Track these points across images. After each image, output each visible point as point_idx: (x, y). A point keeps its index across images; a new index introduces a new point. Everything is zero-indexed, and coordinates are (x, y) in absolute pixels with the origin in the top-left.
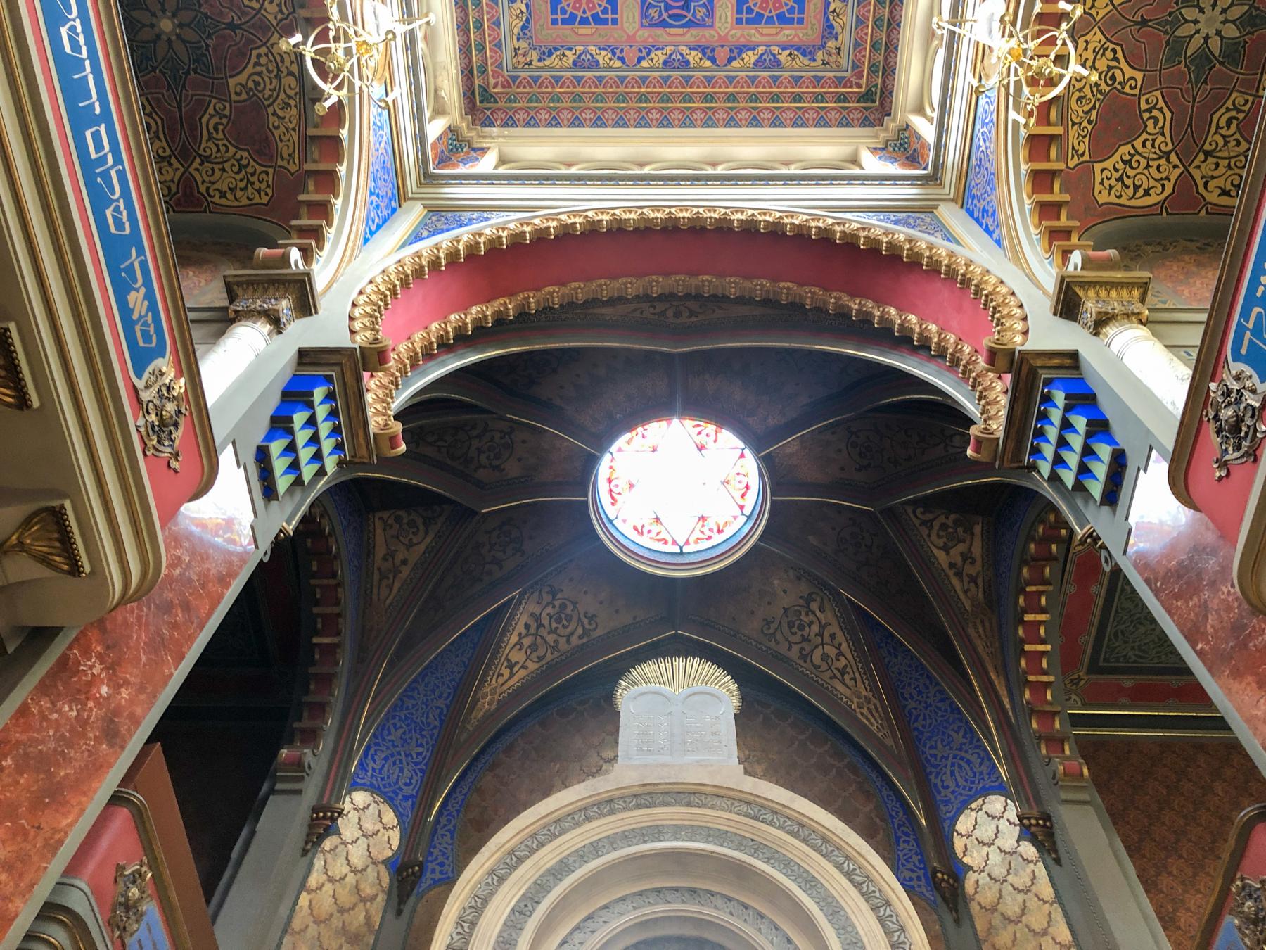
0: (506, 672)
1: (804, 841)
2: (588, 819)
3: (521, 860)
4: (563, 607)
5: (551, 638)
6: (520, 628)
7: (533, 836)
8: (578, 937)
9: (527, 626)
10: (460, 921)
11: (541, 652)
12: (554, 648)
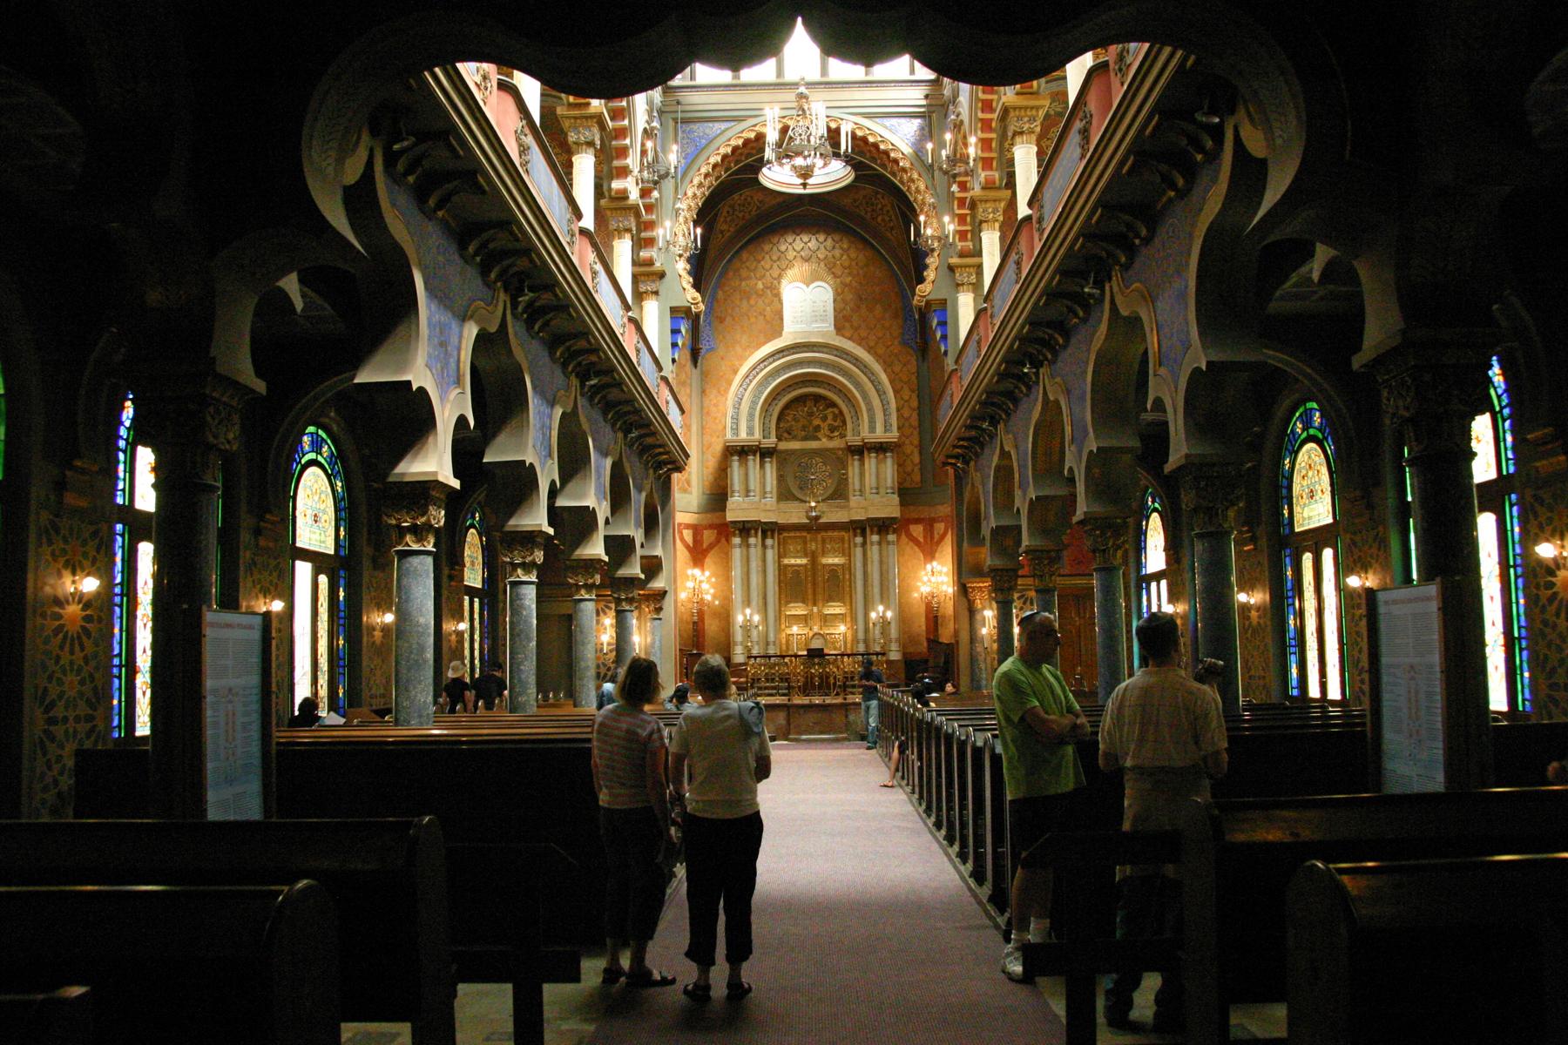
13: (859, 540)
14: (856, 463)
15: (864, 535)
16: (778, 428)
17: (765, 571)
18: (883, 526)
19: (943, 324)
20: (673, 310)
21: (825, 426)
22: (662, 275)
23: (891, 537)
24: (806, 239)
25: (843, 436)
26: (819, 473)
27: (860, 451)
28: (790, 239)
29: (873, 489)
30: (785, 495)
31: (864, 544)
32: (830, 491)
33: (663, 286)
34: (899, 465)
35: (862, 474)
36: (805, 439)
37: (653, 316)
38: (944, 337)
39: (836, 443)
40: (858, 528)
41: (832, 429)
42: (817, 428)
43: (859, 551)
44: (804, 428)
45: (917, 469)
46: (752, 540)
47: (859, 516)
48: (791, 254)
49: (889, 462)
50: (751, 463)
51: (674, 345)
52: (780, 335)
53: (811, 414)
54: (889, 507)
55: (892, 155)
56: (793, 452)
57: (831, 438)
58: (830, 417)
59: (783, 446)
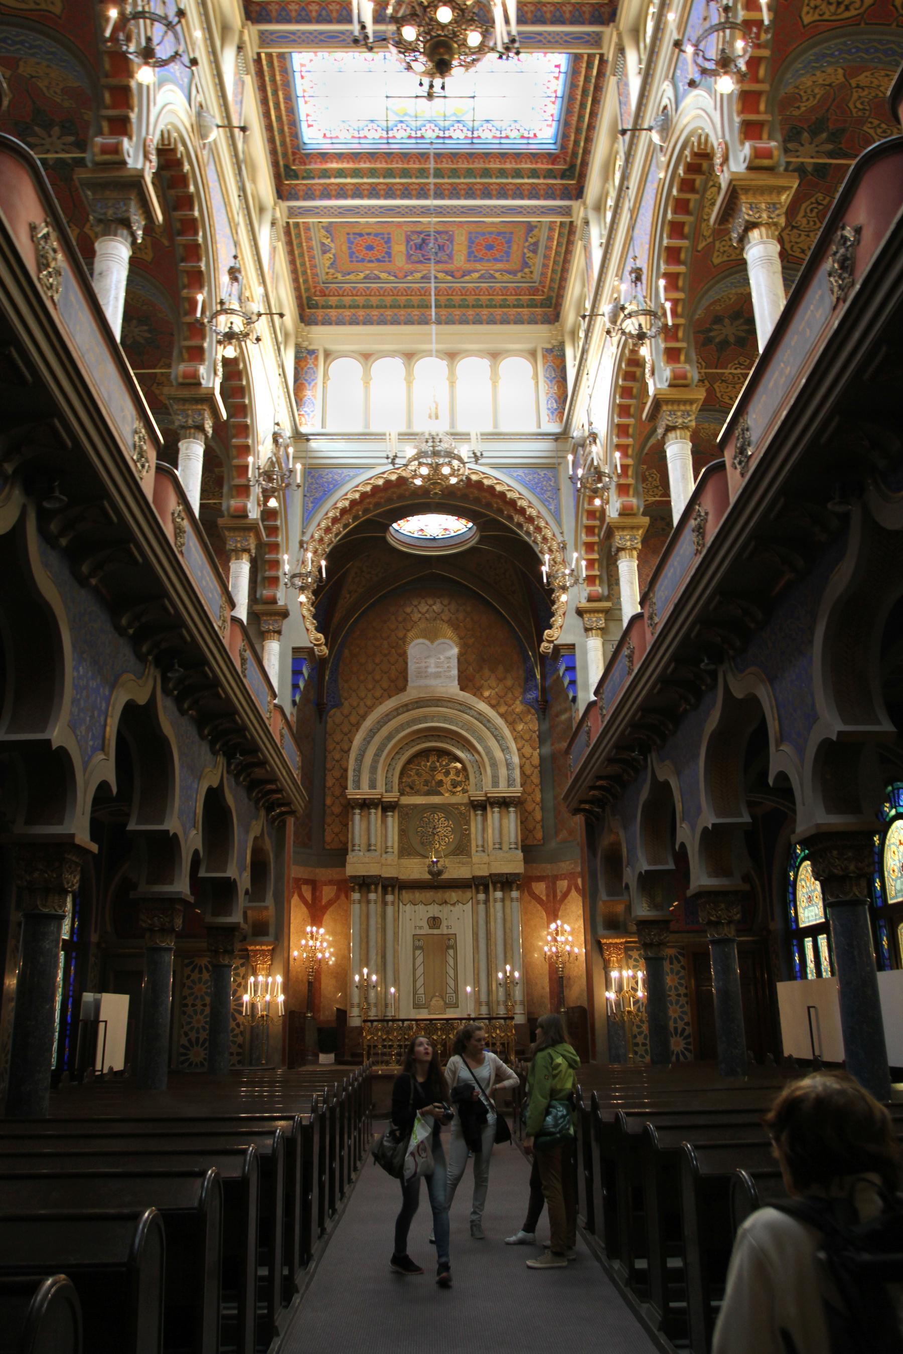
0: (348, 596)
1: (481, 722)
2: (398, 714)
3: (375, 734)
7: (378, 722)
8: (397, 757)
9: (356, 573)
10: (356, 760)
13: (482, 896)
14: (479, 818)
15: (486, 891)
16: (400, 783)
17: (384, 929)
18: (506, 882)
19: (571, 669)
20: (295, 650)
21: (447, 781)
22: (285, 614)
23: (515, 894)
24: (430, 602)
25: (465, 791)
26: (443, 826)
27: (481, 806)
28: (415, 603)
29: (496, 844)
30: (406, 851)
31: (486, 901)
32: (453, 847)
33: (286, 625)
34: (522, 822)
35: (484, 830)
36: (428, 793)
37: (274, 655)
38: (573, 682)
39: (459, 798)
40: (481, 884)
41: (455, 784)
42: (440, 783)
43: (482, 907)
44: (426, 783)
45: (539, 826)
46: (372, 896)
47: (483, 872)
48: (416, 616)
49: (512, 816)
50: (373, 817)
52: (403, 689)
53: (433, 769)
54: (512, 863)
55: (519, 503)
56: (416, 806)
57: (454, 793)
58: (452, 772)
59: (406, 800)
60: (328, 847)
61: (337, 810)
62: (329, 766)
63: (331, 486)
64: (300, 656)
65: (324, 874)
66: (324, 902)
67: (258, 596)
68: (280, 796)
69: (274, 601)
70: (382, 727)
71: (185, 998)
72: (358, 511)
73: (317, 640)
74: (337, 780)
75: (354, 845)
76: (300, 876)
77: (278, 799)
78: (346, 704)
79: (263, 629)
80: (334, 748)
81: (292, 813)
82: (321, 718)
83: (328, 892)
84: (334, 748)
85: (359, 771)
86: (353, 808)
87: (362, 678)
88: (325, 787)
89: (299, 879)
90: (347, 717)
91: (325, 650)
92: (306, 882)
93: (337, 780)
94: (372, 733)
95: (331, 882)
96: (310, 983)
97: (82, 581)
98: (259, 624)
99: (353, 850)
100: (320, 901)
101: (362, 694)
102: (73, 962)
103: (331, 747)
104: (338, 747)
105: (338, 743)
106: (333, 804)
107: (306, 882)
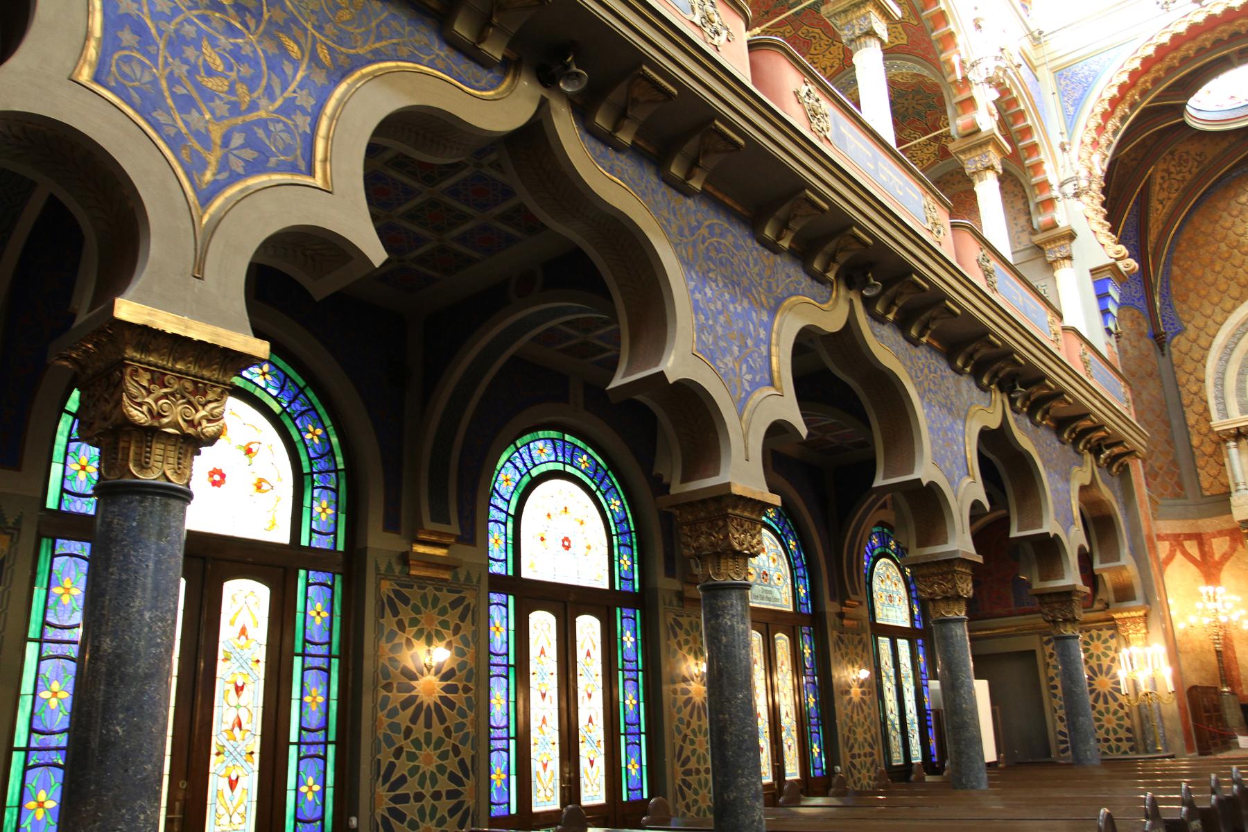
0: (1160, 207)
3: (1232, 350)
4: (1180, 157)
5: (1179, 177)
6: (1159, 180)
7: (1234, 335)
9: (1163, 178)
10: (1216, 385)
11: (1176, 186)
12: (1183, 180)
33: (1075, 248)
37: (1073, 291)
51: (1105, 312)
60: (1208, 493)
61: (1208, 449)
62: (1185, 402)
63: (1090, 79)
64: (1102, 277)
65: (1208, 525)
66: (1217, 557)
67: (1035, 226)
68: (1103, 434)
69: (1054, 226)
70: (1239, 339)
71: (1052, 679)
72: (1133, 96)
73: (1118, 253)
74: (1200, 415)
75: (1237, 485)
76: (1178, 531)
77: (1103, 438)
78: (1190, 327)
79: (1049, 260)
80: (1188, 380)
81: (1131, 453)
82: (1162, 350)
83: (1219, 546)
84: (1188, 380)
85: (1223, 398)
86: (1225, 441)
87: (1203, 293)
88: (1186, 425)
89: (1179, 535)
90: (1194, 341)
91: (1133, 264)
92: (1189, 537)
93: (1200, 415)
94: (1229, 350)
95: (1221, 533)
96: (1218, 652)
97: (682, 188)
98: (1044, 256)
99: (1237, 490)
100: (1212, 556)
101: (1209, 312)
102: (921, 650)
103: (1183, 380)
104: (1192, 378)
105: (1191, 374)
106: (1202, 442)
107: (1189, 537)
